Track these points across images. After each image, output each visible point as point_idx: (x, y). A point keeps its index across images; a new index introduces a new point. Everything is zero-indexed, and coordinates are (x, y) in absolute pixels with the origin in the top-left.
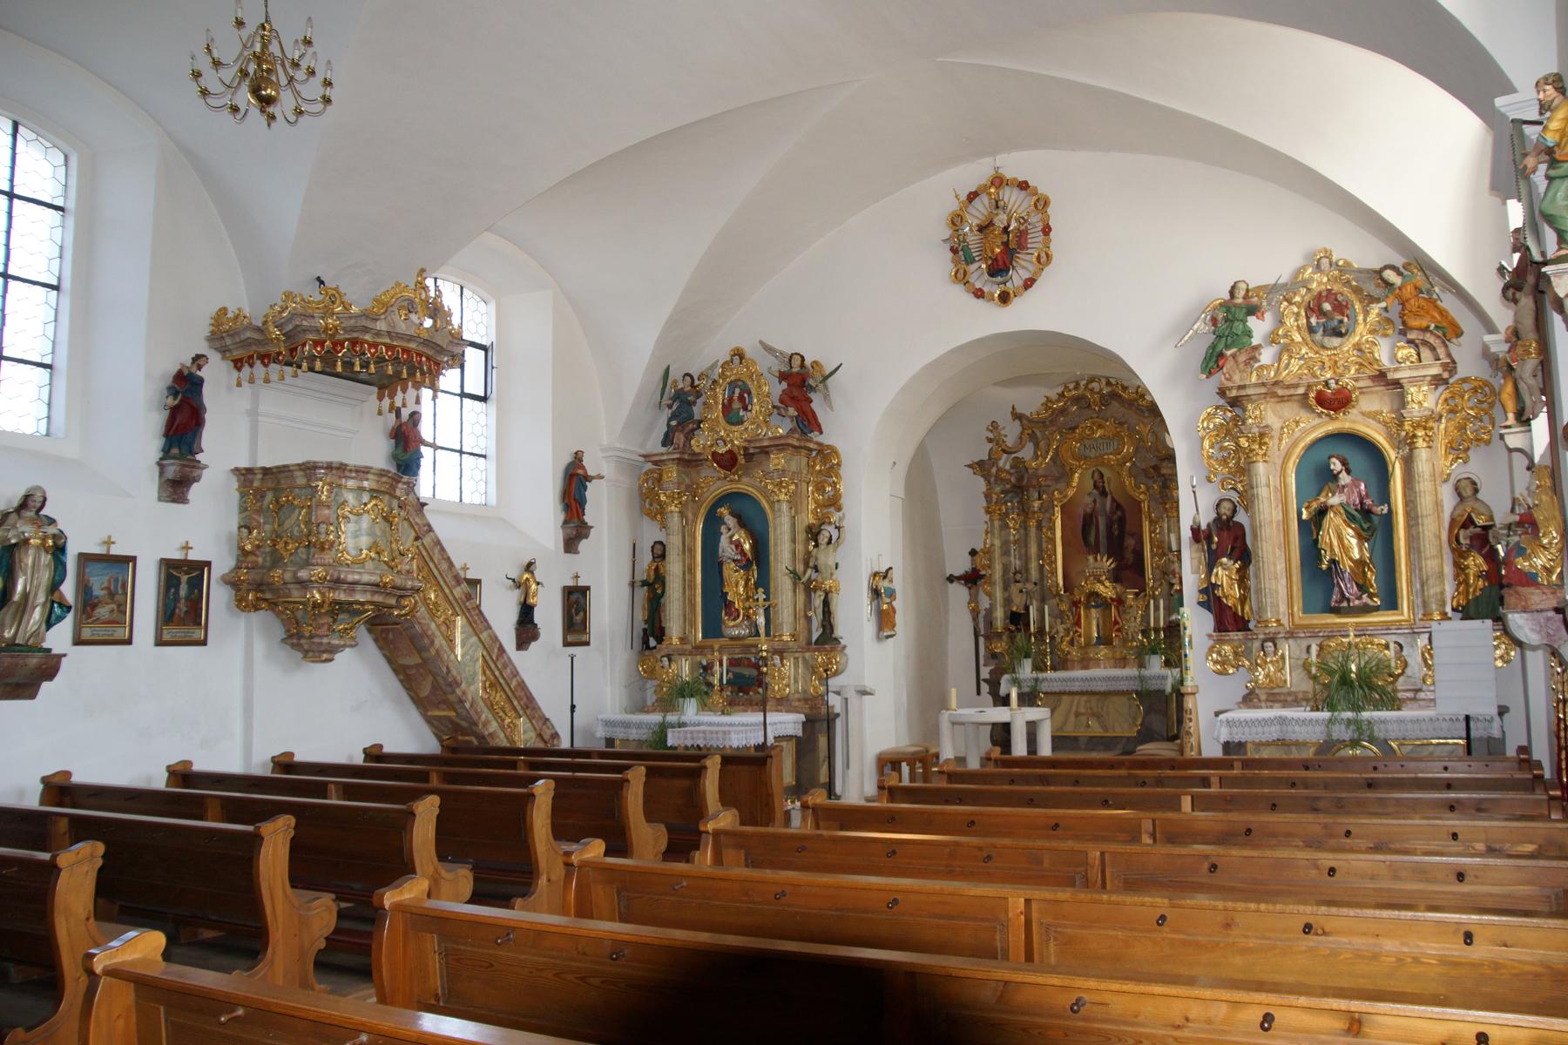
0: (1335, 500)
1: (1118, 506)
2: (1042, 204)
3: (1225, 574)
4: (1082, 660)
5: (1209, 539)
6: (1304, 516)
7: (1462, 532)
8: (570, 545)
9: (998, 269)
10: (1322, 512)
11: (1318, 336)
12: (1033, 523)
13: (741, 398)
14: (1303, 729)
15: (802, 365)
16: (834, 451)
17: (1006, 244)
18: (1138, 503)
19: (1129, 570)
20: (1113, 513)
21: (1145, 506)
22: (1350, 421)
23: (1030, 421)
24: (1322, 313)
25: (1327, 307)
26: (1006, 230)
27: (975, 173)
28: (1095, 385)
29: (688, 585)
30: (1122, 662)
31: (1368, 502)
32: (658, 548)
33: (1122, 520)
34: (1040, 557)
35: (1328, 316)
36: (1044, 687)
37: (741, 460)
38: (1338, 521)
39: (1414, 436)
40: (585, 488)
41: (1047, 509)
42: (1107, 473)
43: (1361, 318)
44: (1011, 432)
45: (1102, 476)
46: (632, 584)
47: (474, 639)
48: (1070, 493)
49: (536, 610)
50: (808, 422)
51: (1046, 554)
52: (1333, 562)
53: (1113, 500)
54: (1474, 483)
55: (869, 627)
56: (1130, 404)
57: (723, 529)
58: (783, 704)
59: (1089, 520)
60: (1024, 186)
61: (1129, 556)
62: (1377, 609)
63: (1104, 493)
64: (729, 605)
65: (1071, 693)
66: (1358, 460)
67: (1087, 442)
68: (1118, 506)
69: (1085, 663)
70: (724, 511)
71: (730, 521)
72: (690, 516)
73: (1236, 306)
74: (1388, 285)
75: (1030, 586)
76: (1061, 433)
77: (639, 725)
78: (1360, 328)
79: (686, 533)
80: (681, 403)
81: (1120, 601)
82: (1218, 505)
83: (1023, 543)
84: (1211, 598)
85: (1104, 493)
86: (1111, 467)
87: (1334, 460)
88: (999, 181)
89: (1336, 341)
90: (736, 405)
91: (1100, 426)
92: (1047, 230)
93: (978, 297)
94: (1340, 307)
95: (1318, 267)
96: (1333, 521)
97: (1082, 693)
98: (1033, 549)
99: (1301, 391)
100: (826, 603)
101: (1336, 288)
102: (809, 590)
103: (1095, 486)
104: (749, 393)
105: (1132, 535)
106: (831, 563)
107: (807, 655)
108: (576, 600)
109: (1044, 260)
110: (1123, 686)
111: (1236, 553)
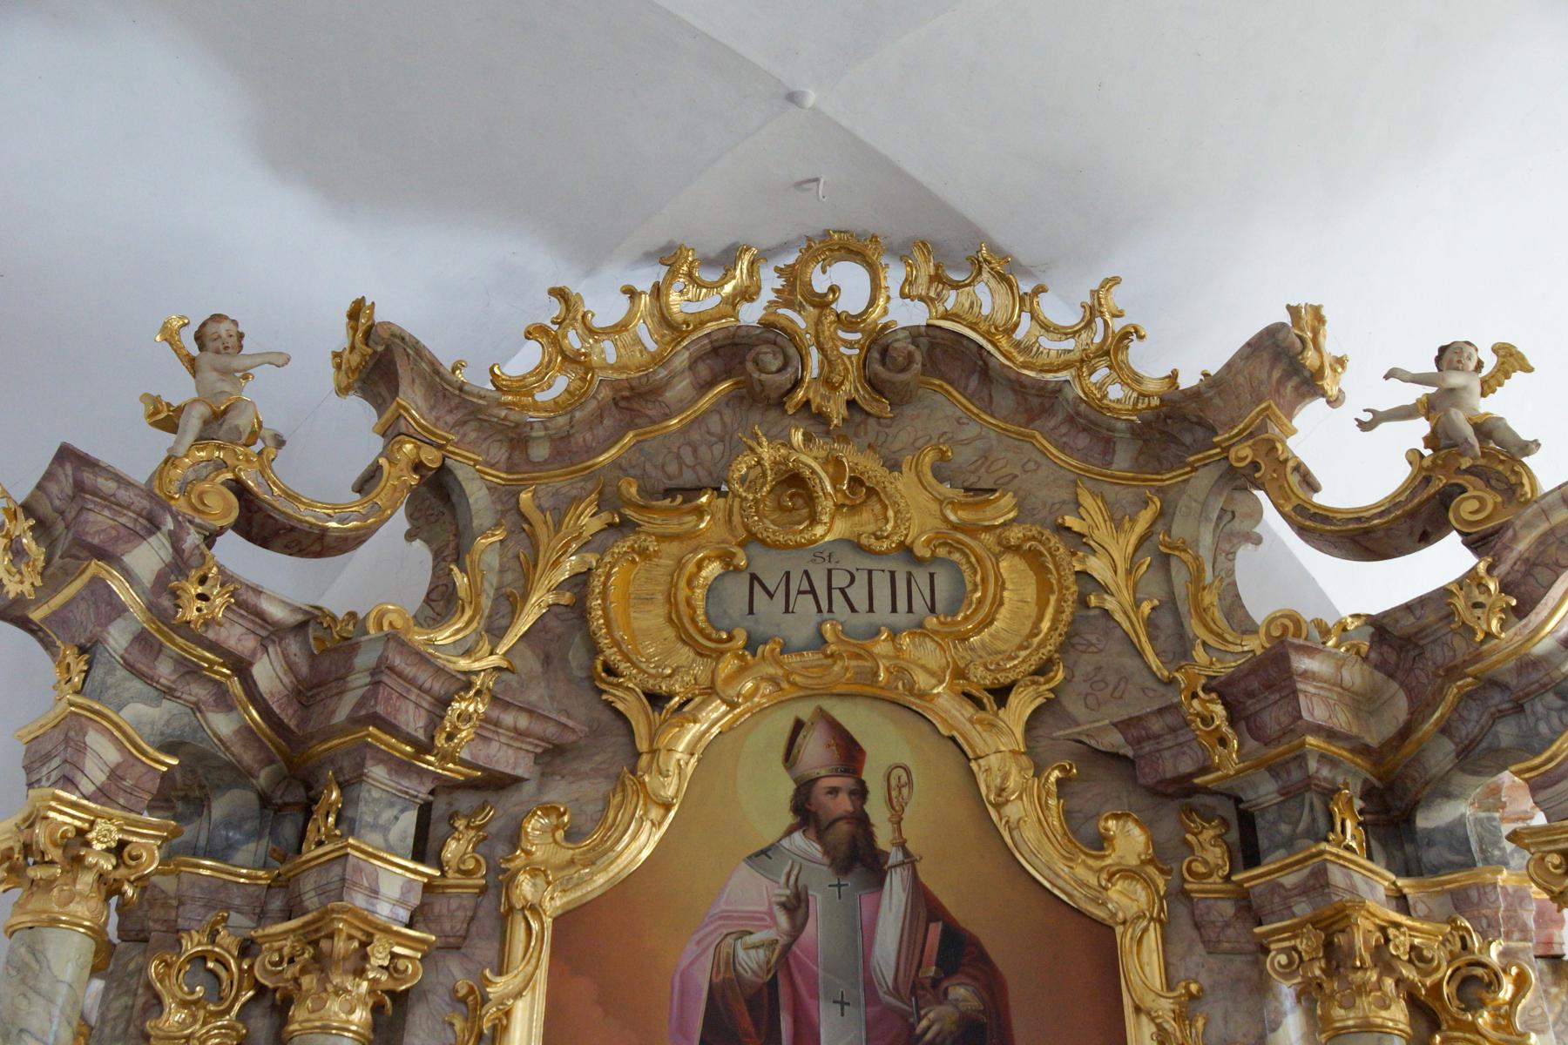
1: (952, 949)
18: (1100, 942)
20: (921, 990)
21: (1144, 965)
23: (444, 388)
28: (848, 284)
41: (468, 922)
42: (884, 743)
44: (326, 446)
45: (850, 753)
48: (640, 845)
53: (925, 906)
56: (1038, 402)
63: (859, 858)
67: (771, 569)
68: (952, 949)
85: (859, 858)
86: (906, 706)
103: (805, 812)
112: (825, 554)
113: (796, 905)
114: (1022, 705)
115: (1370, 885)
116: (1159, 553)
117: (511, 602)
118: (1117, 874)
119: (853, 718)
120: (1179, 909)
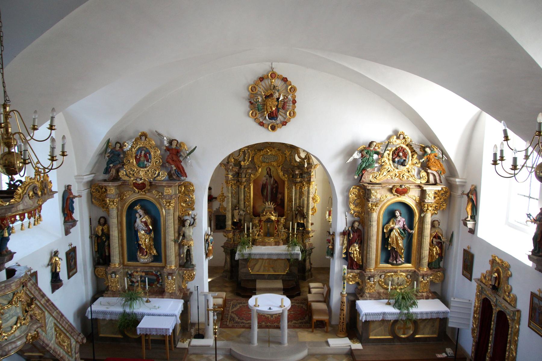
0: (396, 227)
2: (293, 89)
3: (355, 249)
4: (262, 242)
5: (349, 235)
6: (385, 231)
7: (434, 239)
8: (67, 232)
9: (273, 116)
10: (391, 230)
11: (396, 165)
12: (243, 187)
13: (145, 156)
14: (391, 316)
15: (176, 145)
16: (190, 184)
17: (277, 106)
18: (284, 182)
19: (280, 209)
20: (274, 184)
21: (286, 183)
22: (404, 199)
24: (398, 156)
25: (401, 154)
26: (278, 99)
27: (262, 69)
29: (121, 238)
30: (277, 244)
31: (406, 226)
32: (102, 221)
33: (277, 188)
34: (244, 200)
35: (399, 157)
36: (252, 257)
37: (148, 187)
38: (397, 234)
39: (428, 209)
40: (73, 202)
41: (248, 181)
42: (272, 169)
43: (410, 158)
45: (270, 170)
46: (91, 237)
47: (51, 318)
49: (60, 274)
50: (181, 172)
51: (247, 199)
52: (393, 249)
54: (439, 223)
55: (204, 256)
57: (137, 215)
58: (172, 296)
59: (264, 186)
60: (285, 80)
61: (279, 201)
62: (402, 263)
63: (270, 176)
64: (141, 250)
65: (263, 259)
66: (403, 210)
69: (264, 244)
70: (138, 207)
71: (141, 212)
72: (120, 208)
73: (371, 150)
74: (425, 152)
75: (241, 212)
76: (255, 151)
77: (111, 313)
78: (410, 162)
79: (119, 216)
80: (113, 155)
81: (278, 221)
82: (353, 222)
83: (238, 193)
84: (348, 258)
85: (270, 176)
86: (274, 166)
87: (397, 212)
88: (274, 75)
89: (402, 167)
90: (142, 159)
91: (271, 151)
92: (294, 102)
93: (261, 126)
94: (405, 155)
95: (398, 138)
96: (395, 233)
97: (267, 259)
98: (243, 197)
99: (391, 187)
100: (189, 251)
101: (404, 146)
102: (181, 246)
104: (150, 154)
105: (281, 193)
106: (191, 234)
107: (180, 272)
108: (71, 255)
109: (293, 114)
110: (283, 257)
111: (359, 242)
112: (269, 156)
113: (267, 179)
114: (280, 168)
115: (299, 180)
116: (291, 155)
117: (249, 158)
118: (285, 178)
119: (270, 167)
120: (289, 180)
